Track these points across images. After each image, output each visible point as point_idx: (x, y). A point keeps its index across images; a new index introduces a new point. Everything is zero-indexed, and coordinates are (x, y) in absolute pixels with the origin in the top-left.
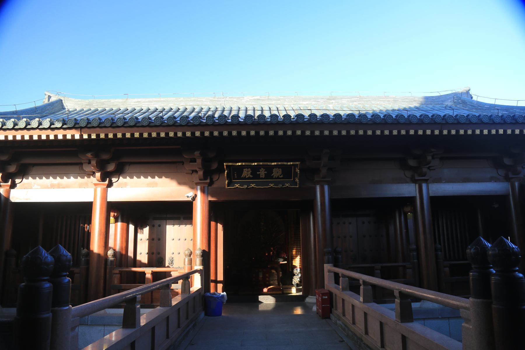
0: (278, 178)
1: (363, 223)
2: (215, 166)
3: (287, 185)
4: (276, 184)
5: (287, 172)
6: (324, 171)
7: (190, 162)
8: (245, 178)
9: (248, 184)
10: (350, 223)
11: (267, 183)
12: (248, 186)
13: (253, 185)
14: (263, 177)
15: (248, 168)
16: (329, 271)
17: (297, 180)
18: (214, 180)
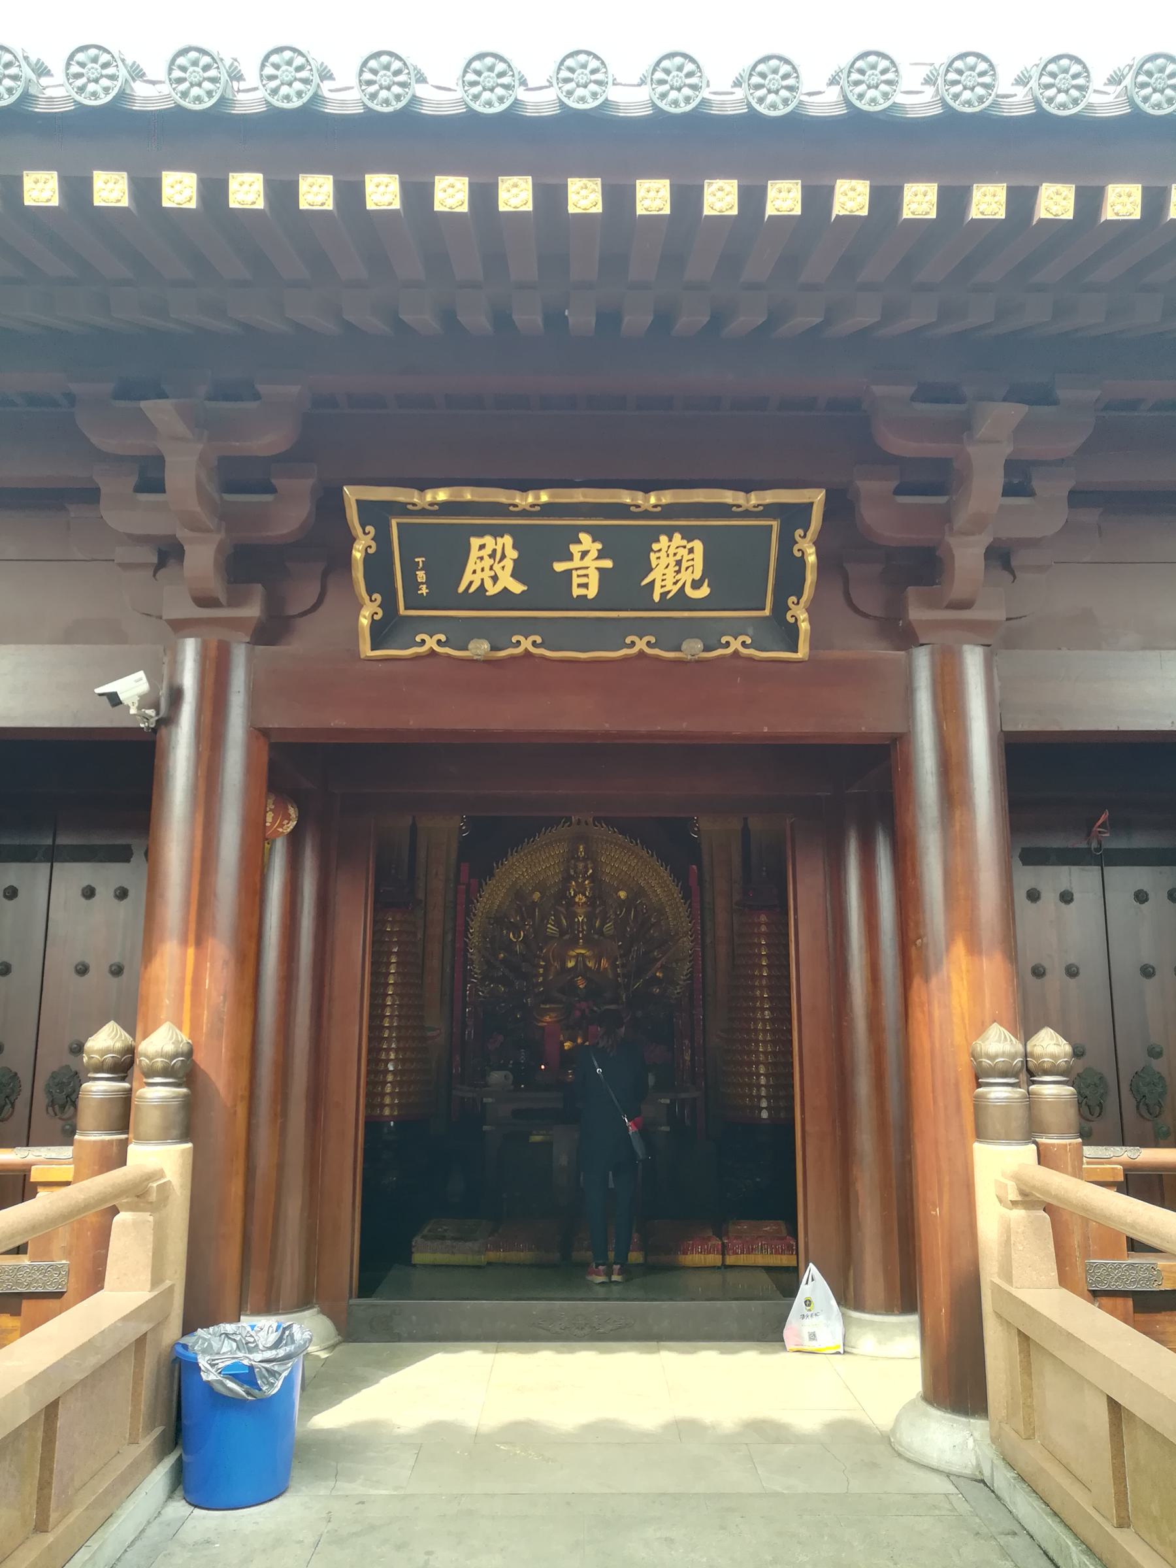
0: (680, 600)
1: (1141, 897)
2: (289, 515)
3: (736, 645)
4: (670, 634)
5: (734, 568)
6: (967, 557)
7: (139, 489)
8: (479, 598)
9: (498, 633)
10: (1066, 897)
11: (616, 633)
12: (494, 648)
13: (526, 644)
14: (592, 592)
15: (497, 532)
16: (1029, 1198)
17: (800, 615)
18: (293, 610)
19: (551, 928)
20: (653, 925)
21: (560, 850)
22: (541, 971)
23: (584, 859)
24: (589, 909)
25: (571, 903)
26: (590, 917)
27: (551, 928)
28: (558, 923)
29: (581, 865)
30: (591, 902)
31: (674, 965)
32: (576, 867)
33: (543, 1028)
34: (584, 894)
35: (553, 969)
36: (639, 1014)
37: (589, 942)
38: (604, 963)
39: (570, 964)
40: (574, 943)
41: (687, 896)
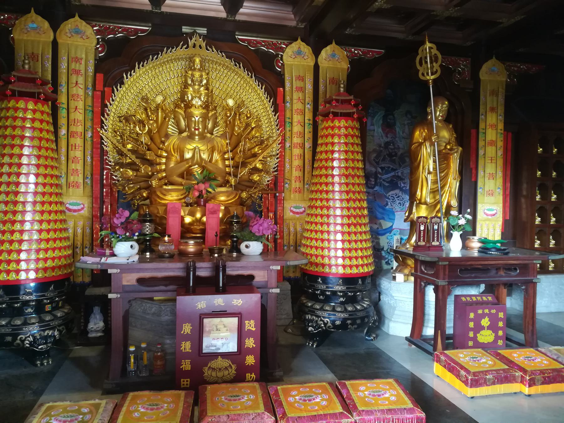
19: (171, 129)
20: (253, 129)
21: (178, 67)
22: (164, 160)
23: (199, 70)
24: (204, 111)
25: (188, 106)
26: (205, 117)
27: (171, 129)
28: (178, 124)
29: (197, 74)
30: (206, 106)
31: (269, 159)
32: (193, 75)
33: (165, 205)
34: (200, 98)
35: (174, 159)
36: (244, 195)
37: (202, 137)
38: (216, 156)
39: (188, 155)
40: (191, 137)
41: (276, 111)
